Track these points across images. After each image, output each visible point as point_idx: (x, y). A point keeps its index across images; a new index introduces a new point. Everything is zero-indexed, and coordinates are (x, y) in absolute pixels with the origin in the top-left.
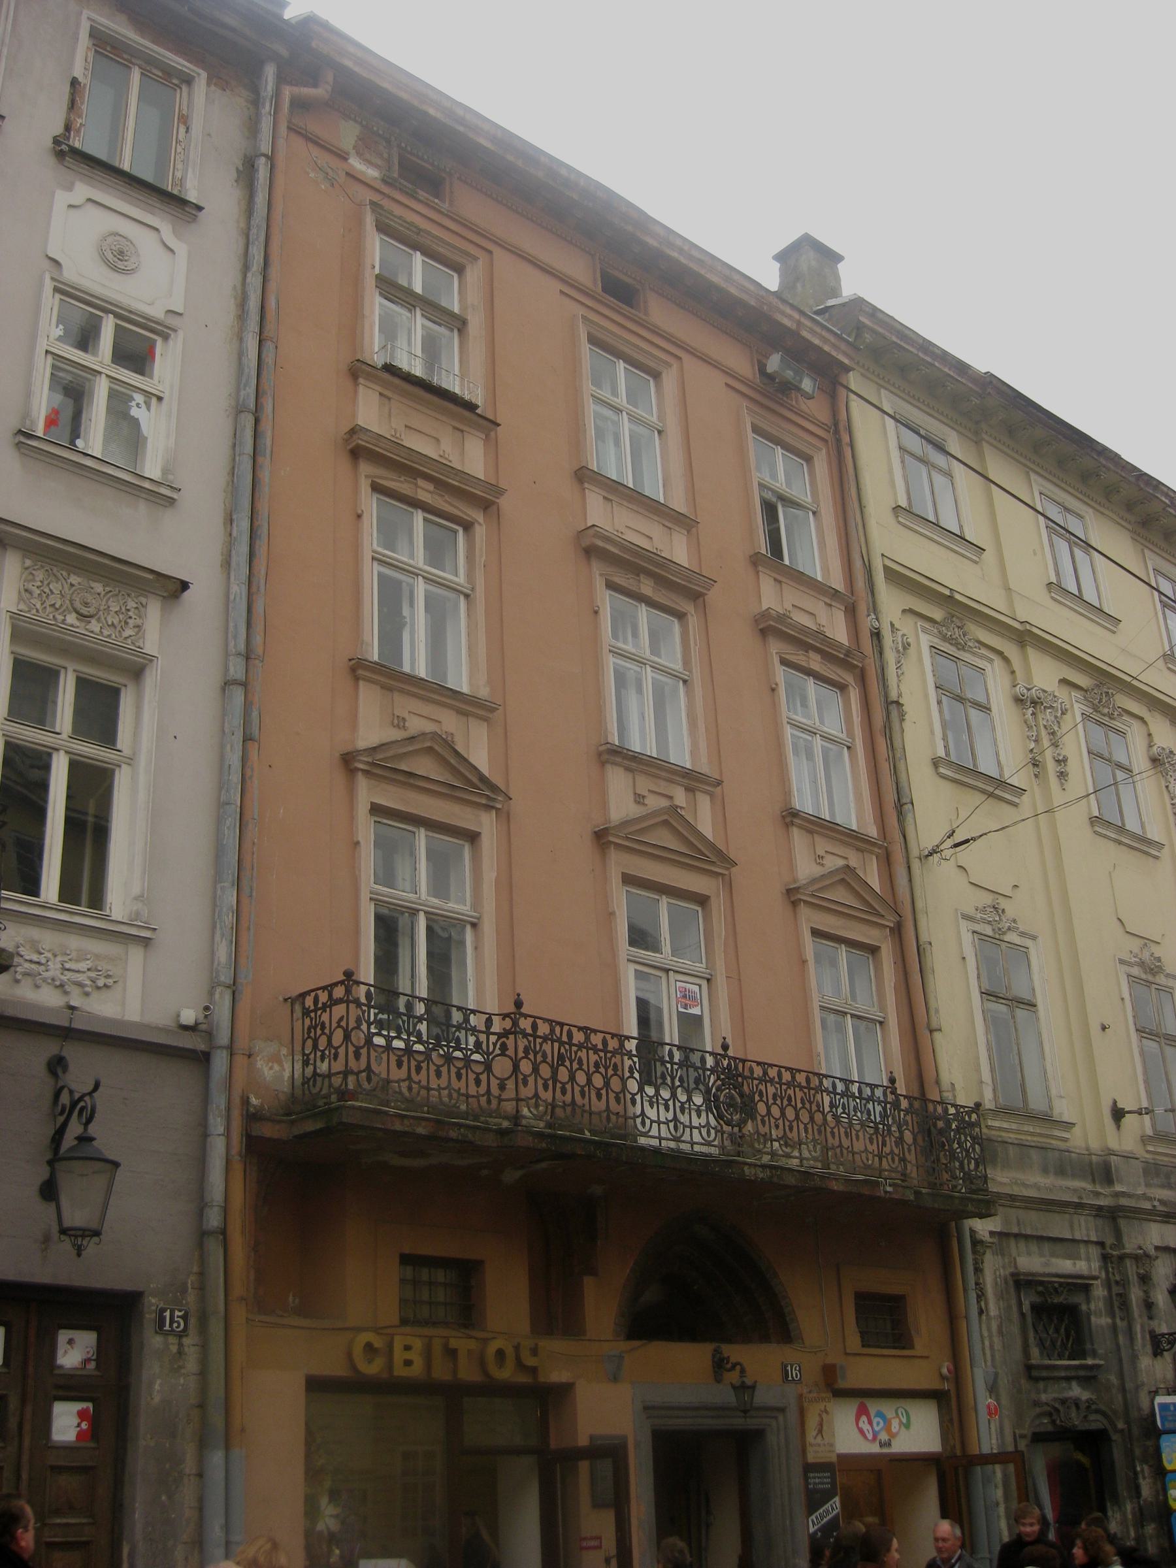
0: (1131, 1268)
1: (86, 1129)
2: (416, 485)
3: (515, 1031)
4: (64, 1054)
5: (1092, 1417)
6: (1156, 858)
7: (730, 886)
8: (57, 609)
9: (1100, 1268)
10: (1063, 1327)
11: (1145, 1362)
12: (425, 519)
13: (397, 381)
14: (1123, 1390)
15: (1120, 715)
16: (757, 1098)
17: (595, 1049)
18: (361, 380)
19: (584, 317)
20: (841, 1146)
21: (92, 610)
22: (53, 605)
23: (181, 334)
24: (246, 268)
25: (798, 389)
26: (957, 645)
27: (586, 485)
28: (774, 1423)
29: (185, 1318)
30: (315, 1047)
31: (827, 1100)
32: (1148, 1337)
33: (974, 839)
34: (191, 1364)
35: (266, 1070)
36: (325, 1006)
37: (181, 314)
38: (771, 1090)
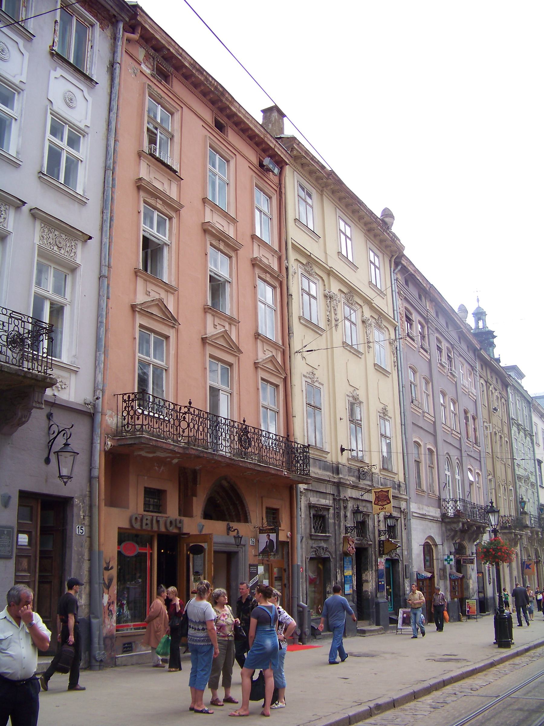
2: (157, 201)
3: (188, 412)
4: (52, 412)
5: (327, 553)
6: (360, 358)
8: (51, 244)
12: (158, 215)
13: (154, 160)
14: (335, 544)
15: (355, 304)
18: (142, 158)
19: (209, 137)
22: (50, 242)
25: (273, 172)
27: (206, 204)
31: (263, 439)
35: (108, 420)
37: (89, 127)
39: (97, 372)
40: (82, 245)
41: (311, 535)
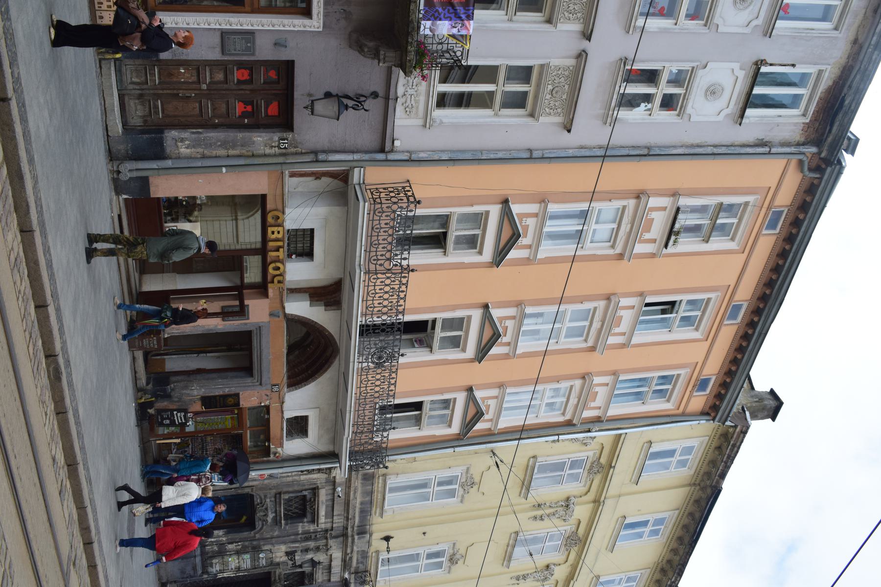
0: (322, 542)
1: (350, 107)
7: (471, 361)
9: (322, 528)
10: (297, 511)
11: (283, 548)
14: (272, 538)
16: (383, 369)
17: (398, 302)
18: (672, 198)
20: (367, 404)
21: (554, 95)
23: (681, 121)
24: (715, 146)
26: (590, 469)
28: (255, 381)
29: (285, 148)
30: (391, 192)
32: (294, 549)
33: (499, 470)
34: (268, 151)
36: (406, 194)
38: (387, 375)
39: (429, 153)
40: (559, 123)
41: (280, 493)
